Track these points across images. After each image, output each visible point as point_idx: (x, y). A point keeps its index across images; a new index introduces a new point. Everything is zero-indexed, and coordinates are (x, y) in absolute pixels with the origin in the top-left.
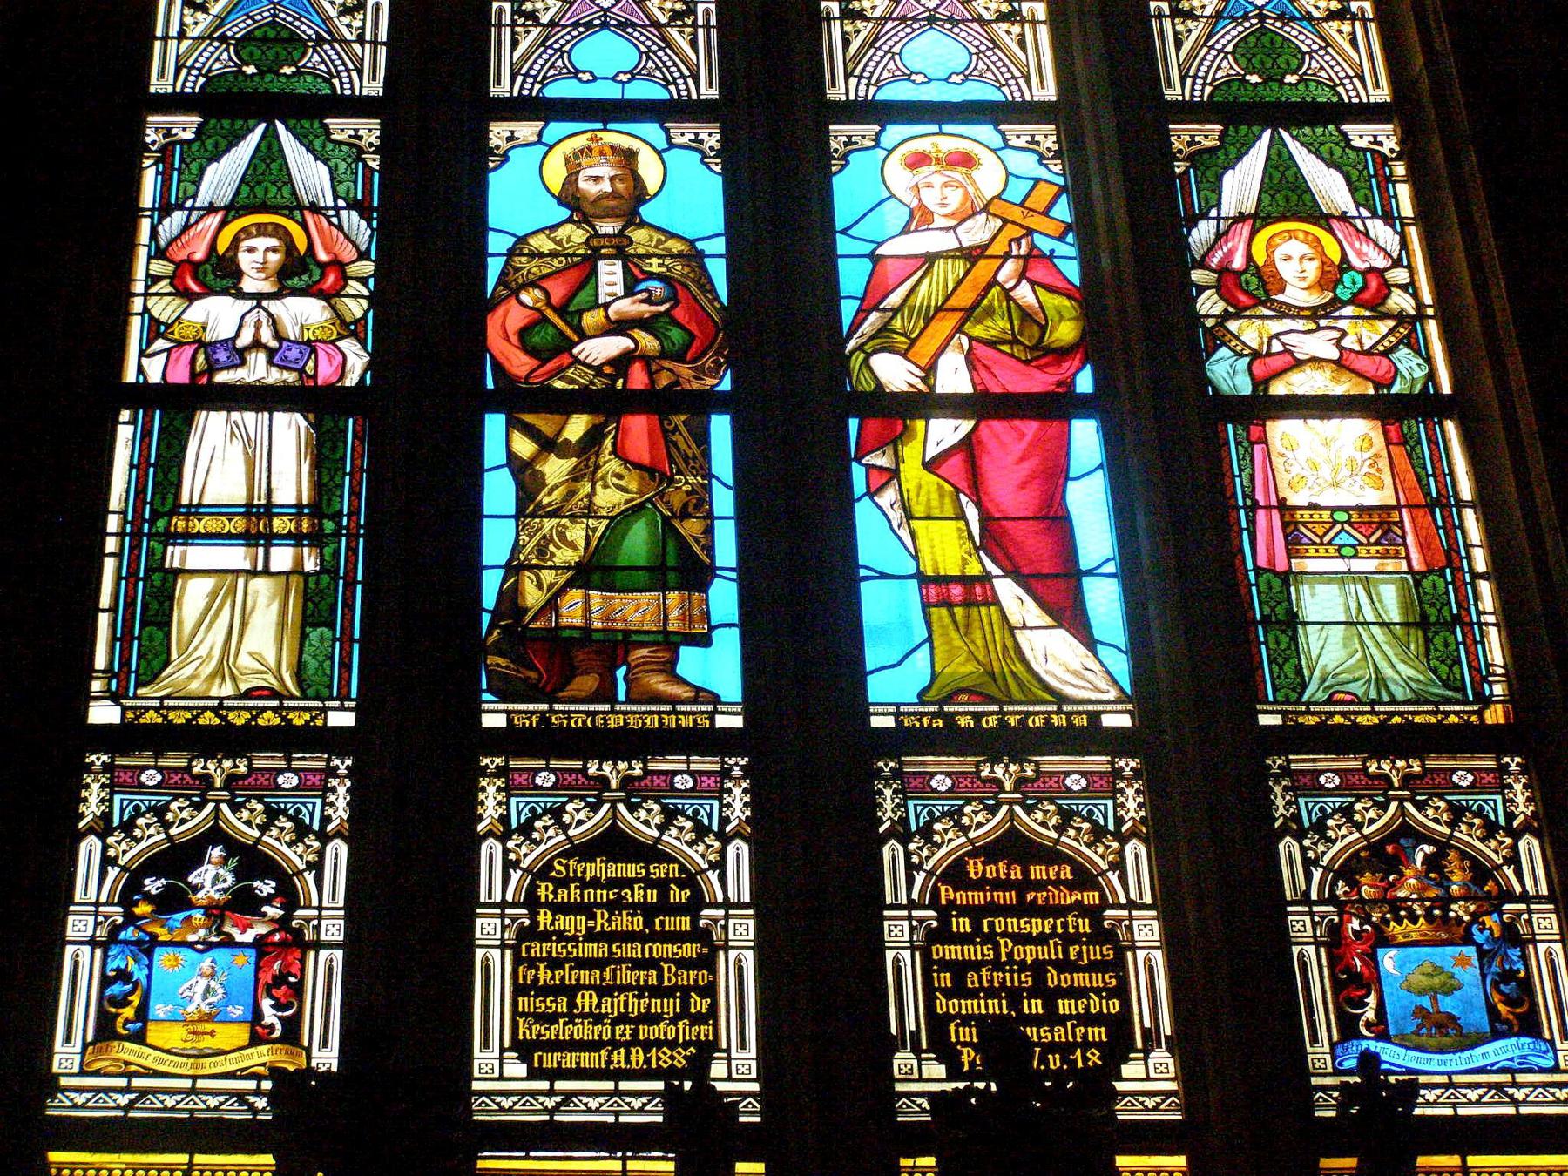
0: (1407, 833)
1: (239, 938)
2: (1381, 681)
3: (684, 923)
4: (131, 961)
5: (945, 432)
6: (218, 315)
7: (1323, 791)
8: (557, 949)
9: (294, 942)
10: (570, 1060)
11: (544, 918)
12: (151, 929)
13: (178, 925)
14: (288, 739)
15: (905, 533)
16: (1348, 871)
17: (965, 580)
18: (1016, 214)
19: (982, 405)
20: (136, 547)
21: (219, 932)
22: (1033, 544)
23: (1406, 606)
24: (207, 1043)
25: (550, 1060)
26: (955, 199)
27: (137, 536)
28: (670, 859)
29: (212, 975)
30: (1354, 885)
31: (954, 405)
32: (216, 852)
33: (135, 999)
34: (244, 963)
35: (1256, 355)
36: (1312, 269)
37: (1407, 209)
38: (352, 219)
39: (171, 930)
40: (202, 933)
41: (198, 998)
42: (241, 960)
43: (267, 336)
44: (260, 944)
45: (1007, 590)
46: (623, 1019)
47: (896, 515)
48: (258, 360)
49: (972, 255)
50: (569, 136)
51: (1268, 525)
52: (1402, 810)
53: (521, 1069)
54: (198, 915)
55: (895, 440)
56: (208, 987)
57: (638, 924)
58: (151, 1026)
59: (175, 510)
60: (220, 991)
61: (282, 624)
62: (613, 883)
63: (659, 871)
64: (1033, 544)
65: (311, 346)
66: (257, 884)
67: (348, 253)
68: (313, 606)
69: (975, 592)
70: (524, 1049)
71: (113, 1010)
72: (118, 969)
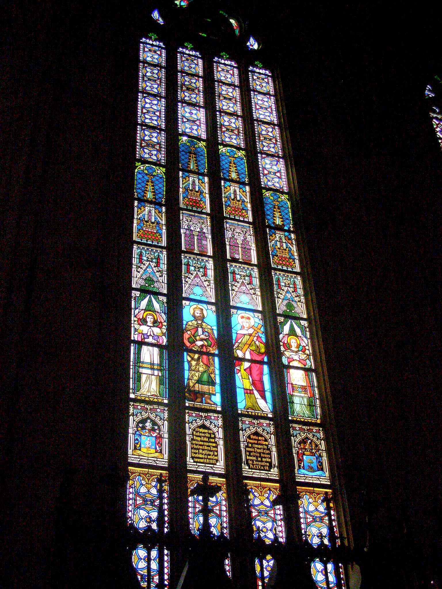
0: (307, 438)
2: (304, 413)
3: (213, 440)
5: (247, 365)
6: (144, 329)
7: (296, 430)
8: (197, 442)
9: (159, 437)
10: (199, 460)
11: (195, 437)
14: (159, 404)
15: (242, 381)
16: (300, 443)
17: (250, 390)
18: (256, 329)
19: (251, 361)
20: (135, 368)
22: (259, 385)
23: (308, 403)
25: (196, 460)
26: (248, 326)
27: (135, 366)
28: (211, 430)
30: (300, 445)
31: (248, 361)
32: (149, 421)
34: (154, 439)
35: (288, 358)
36: (296, 344)
37: (308, 337)
38: (163, 314)
43: (152, 334)
44: (156, 437)
45: (255, 392)
46: (205, 454)
47: (240, 378)
48: (151, 338)
49: (250, 335)
50: (194, 305)
51: (290, 386)
52: (307, 435)
53: (192, 461)
54: (147, 431)
55: (240, 365)
57: (207, 440)
59: (140, 362)
61: (157, 384)
62: (204, 433)
63: (210, 431)
64: (259, 385)
65: (158, 336)
67: (163, 321)
68: (161, 382)
69: (251, 392)
70: (193, 458)
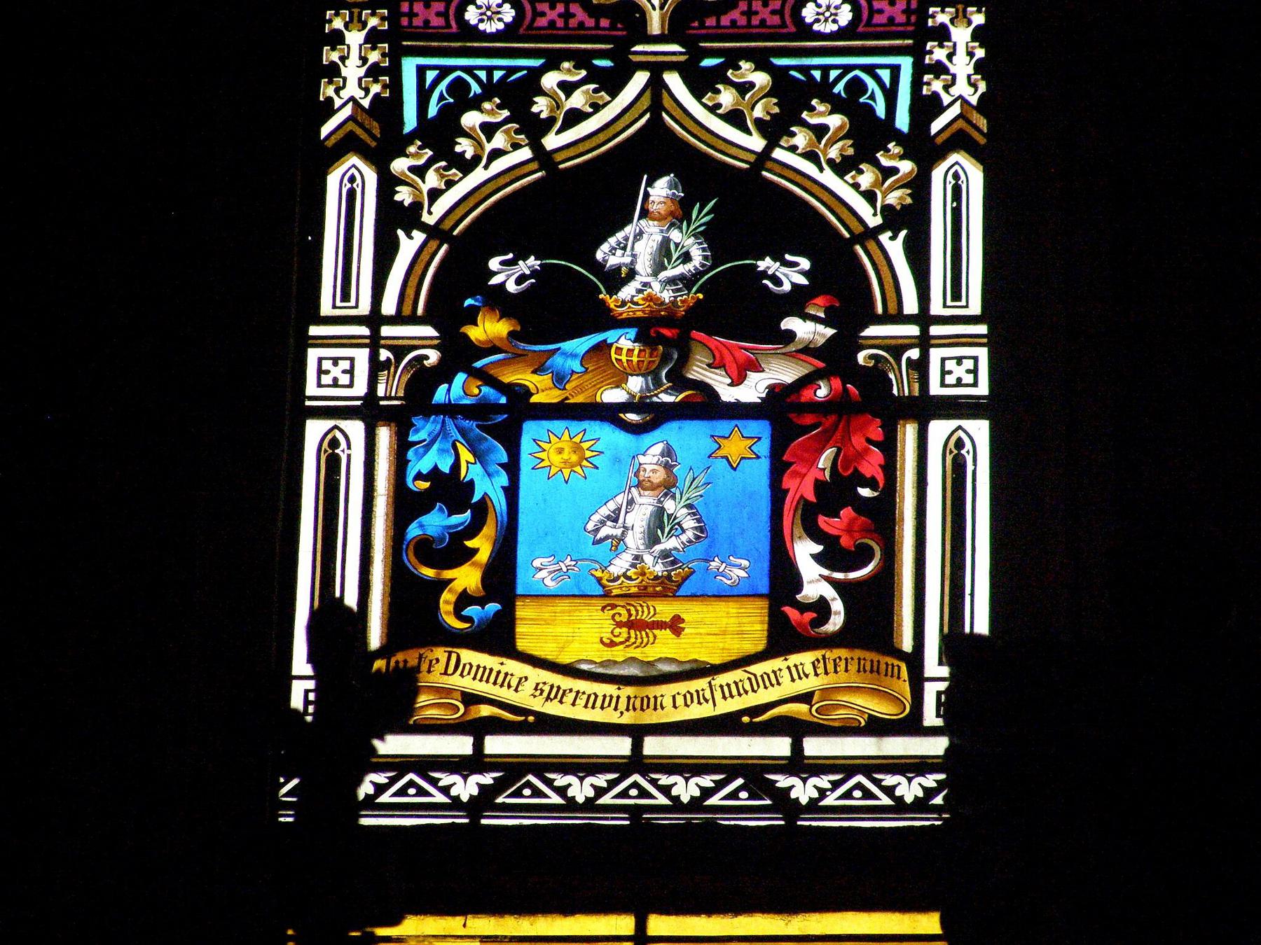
1: (728, 394)
4: (466, 455)
12: (508, 378)
13: (576, 365)
21: (679, 381)
24: (663, 648)
29: (668, 487)
33: (483, 545)
39: (560, 380)
40: (636, 384)
41: (635, 541)
42: (735, 447)
44: (779, 408)
54: (624, 341)
56: (660, 512)
58: (523, 611)
60: (689, 523)
66: (766, 264)
71: (429, 572)
72: (435, 473)
